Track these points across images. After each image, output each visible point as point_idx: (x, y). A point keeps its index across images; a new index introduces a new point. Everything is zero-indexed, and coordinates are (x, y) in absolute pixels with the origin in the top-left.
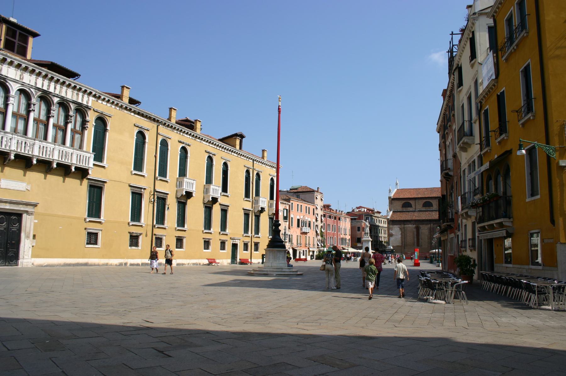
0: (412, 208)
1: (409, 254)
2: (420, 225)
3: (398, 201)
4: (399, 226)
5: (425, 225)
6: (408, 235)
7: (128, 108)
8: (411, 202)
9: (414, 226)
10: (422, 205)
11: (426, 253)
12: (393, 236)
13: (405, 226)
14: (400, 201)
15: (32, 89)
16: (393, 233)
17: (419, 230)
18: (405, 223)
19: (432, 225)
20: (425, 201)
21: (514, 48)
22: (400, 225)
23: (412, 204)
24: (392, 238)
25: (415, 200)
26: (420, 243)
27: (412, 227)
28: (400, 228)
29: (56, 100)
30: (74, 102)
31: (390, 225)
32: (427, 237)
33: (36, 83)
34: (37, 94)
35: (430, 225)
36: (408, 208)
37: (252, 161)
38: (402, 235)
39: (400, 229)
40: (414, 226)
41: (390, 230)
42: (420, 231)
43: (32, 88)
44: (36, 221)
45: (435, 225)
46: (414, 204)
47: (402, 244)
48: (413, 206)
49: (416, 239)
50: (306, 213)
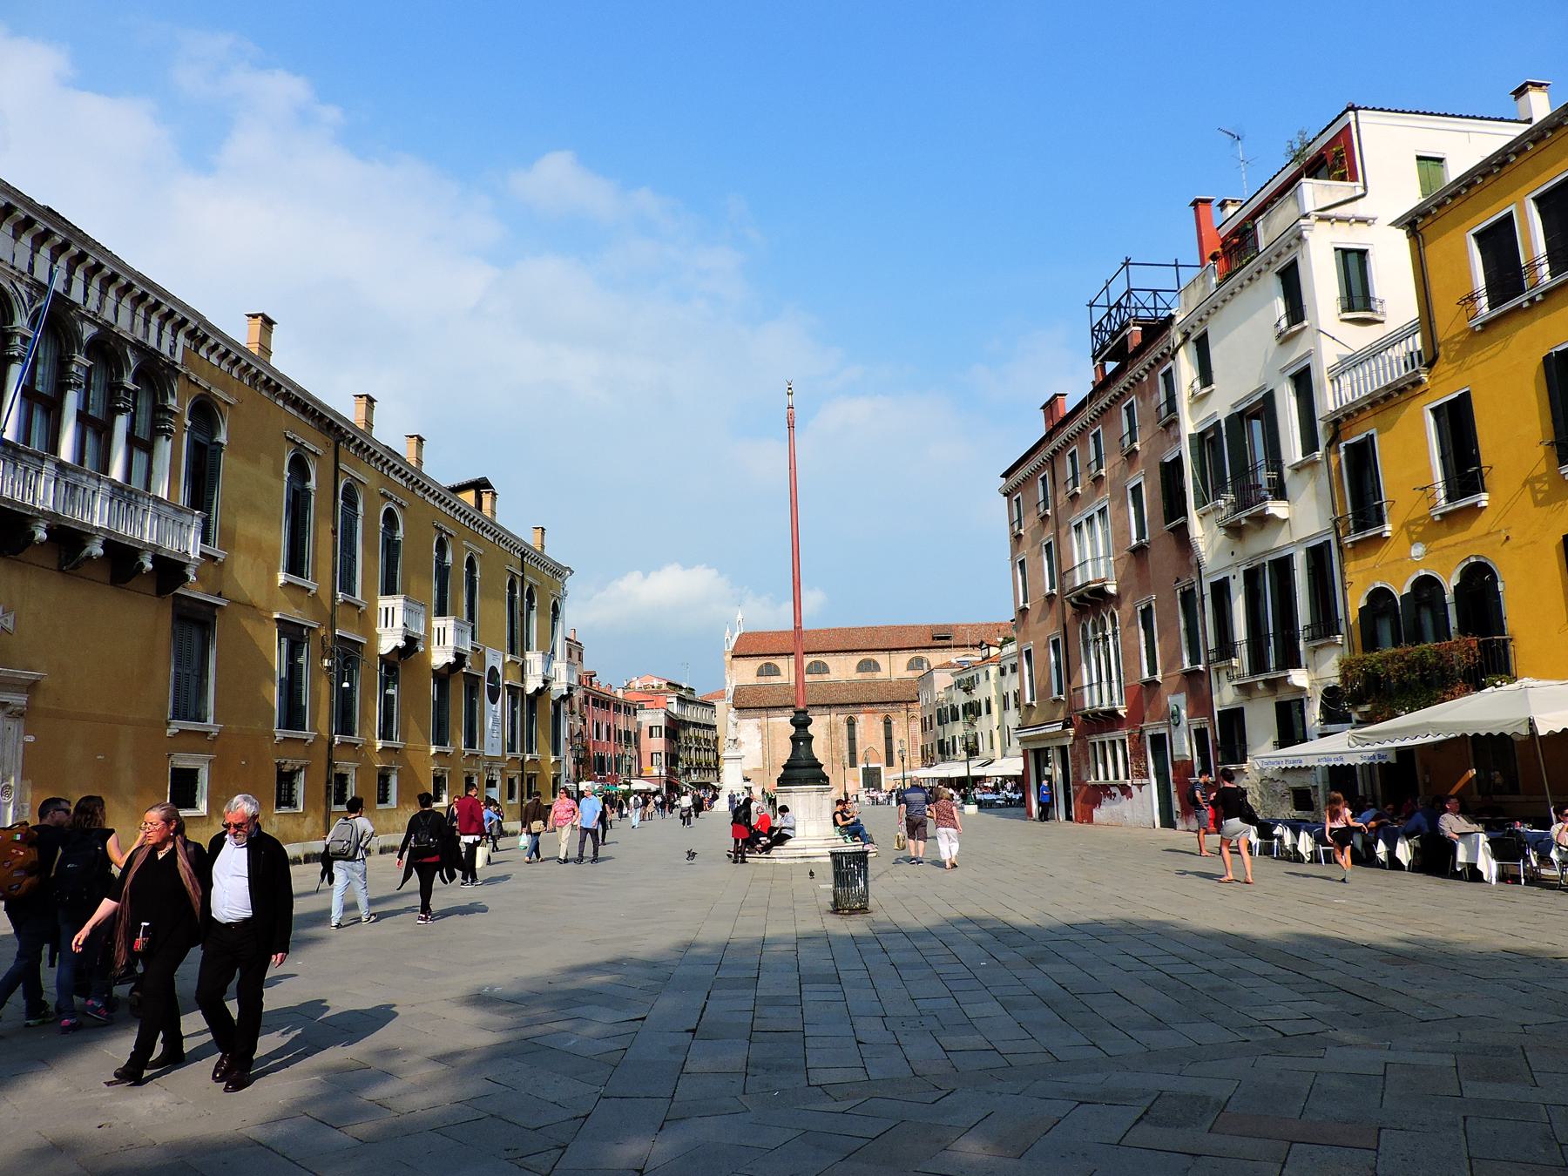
7: (273, 383)
15: (18, 285)
21: (1532, 300)
29: (88, 331)
30: (139, 347)
32: (822, 746)
33: (31, 267)
34: (34, 304)
37: (520, 556)
43: (21, 280)
44: (30, 739)
48: (782, 672)
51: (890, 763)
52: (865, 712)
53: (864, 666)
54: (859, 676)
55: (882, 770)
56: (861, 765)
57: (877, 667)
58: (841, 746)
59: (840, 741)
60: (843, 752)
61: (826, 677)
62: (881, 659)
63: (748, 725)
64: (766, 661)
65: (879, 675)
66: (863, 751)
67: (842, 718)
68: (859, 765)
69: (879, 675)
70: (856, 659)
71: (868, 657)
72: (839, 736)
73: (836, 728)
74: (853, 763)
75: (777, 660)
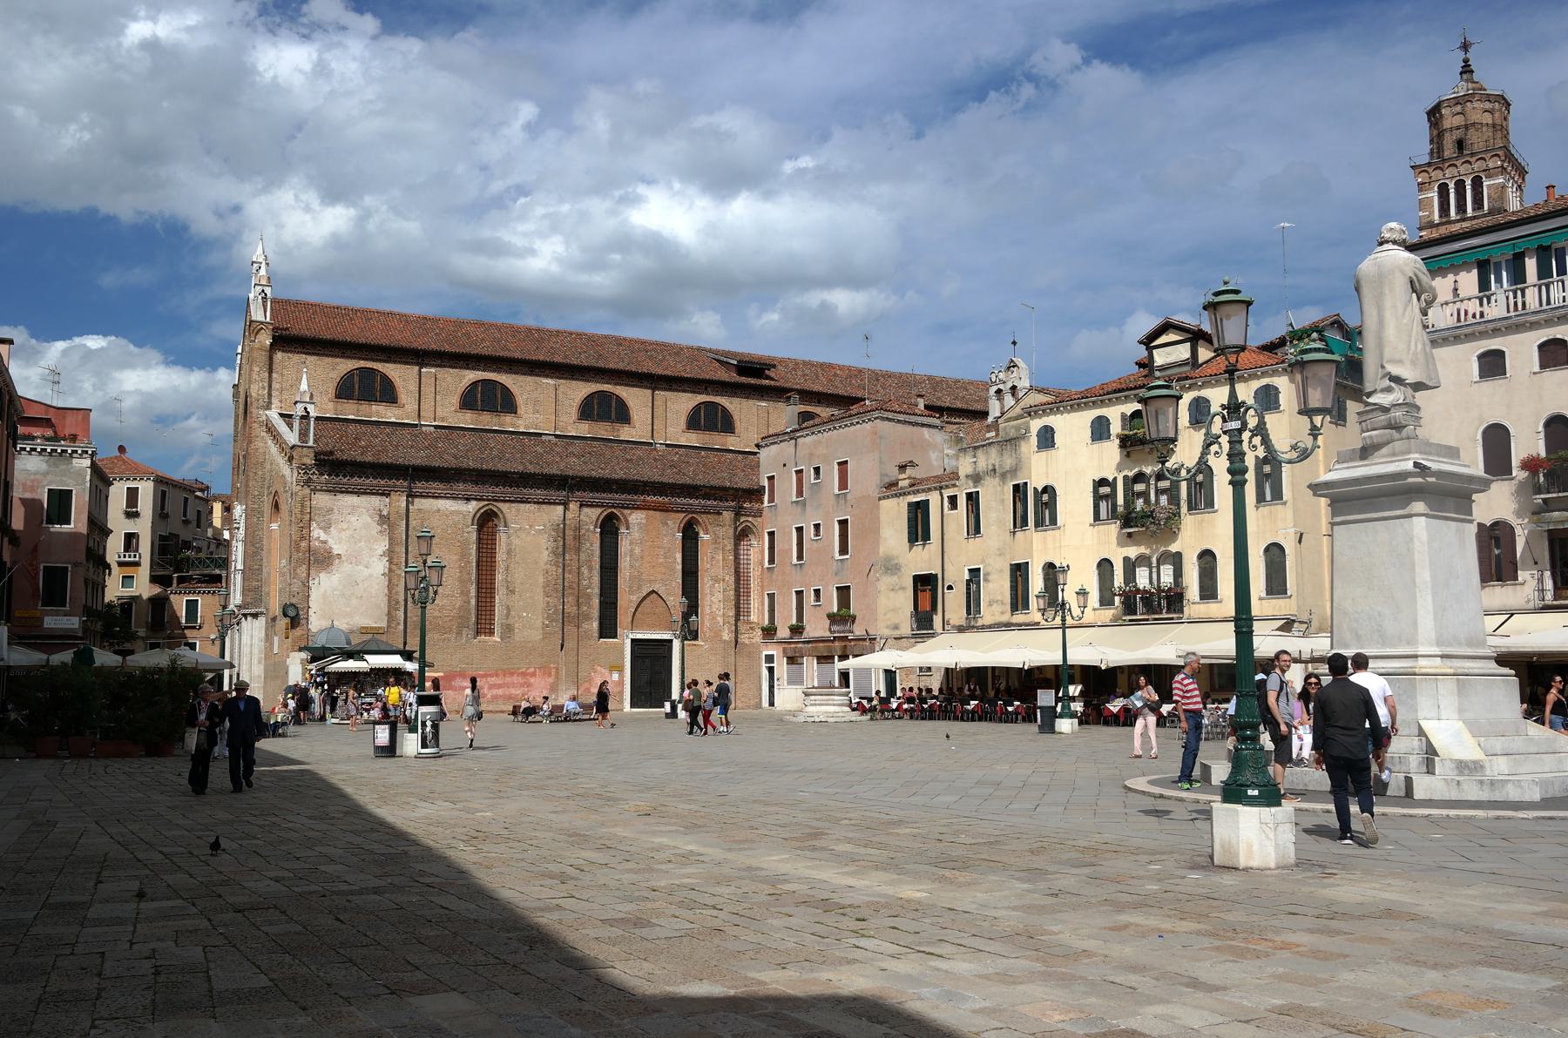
0: (397, 411)
2: (504, 507)
4: (375, 501)
5: (533, 507)
8: (393, 371)
9: (473, 506)
10: (455, 400)
11: (533, 675)
13: (419, 503)
16: (331, 542)
18: (419, 486)
20: (472, 376)
22: (382, 494)
23: (398, 382)
24: (322, 575)
27: (452, 513)
28: (381, 516)
31: (315, 491)
32: (541, 580)
35: (560, 508)
38: (390, 561)
39: (384, 519)
41: (314, 525)
45: (586, 510)
46: (414, 387)
47: (390, 616)
48: (403, 397)
51: (691, 634)
53: (593, 409)
55: (676, 645)
57: (622, 414)
58: (585, 583)
59: (585, 570)
60: (589, 597)
61: (508, 422)
62: (635, 398)
63: (354, 508)
64: (363, 364)
65: (626, 433)
66: (636, 598)
67: (592, 515)
69: (626, 433)
70: (580, 390)
72: (583, 556)
73: (575, 538)
74: (608, 628)
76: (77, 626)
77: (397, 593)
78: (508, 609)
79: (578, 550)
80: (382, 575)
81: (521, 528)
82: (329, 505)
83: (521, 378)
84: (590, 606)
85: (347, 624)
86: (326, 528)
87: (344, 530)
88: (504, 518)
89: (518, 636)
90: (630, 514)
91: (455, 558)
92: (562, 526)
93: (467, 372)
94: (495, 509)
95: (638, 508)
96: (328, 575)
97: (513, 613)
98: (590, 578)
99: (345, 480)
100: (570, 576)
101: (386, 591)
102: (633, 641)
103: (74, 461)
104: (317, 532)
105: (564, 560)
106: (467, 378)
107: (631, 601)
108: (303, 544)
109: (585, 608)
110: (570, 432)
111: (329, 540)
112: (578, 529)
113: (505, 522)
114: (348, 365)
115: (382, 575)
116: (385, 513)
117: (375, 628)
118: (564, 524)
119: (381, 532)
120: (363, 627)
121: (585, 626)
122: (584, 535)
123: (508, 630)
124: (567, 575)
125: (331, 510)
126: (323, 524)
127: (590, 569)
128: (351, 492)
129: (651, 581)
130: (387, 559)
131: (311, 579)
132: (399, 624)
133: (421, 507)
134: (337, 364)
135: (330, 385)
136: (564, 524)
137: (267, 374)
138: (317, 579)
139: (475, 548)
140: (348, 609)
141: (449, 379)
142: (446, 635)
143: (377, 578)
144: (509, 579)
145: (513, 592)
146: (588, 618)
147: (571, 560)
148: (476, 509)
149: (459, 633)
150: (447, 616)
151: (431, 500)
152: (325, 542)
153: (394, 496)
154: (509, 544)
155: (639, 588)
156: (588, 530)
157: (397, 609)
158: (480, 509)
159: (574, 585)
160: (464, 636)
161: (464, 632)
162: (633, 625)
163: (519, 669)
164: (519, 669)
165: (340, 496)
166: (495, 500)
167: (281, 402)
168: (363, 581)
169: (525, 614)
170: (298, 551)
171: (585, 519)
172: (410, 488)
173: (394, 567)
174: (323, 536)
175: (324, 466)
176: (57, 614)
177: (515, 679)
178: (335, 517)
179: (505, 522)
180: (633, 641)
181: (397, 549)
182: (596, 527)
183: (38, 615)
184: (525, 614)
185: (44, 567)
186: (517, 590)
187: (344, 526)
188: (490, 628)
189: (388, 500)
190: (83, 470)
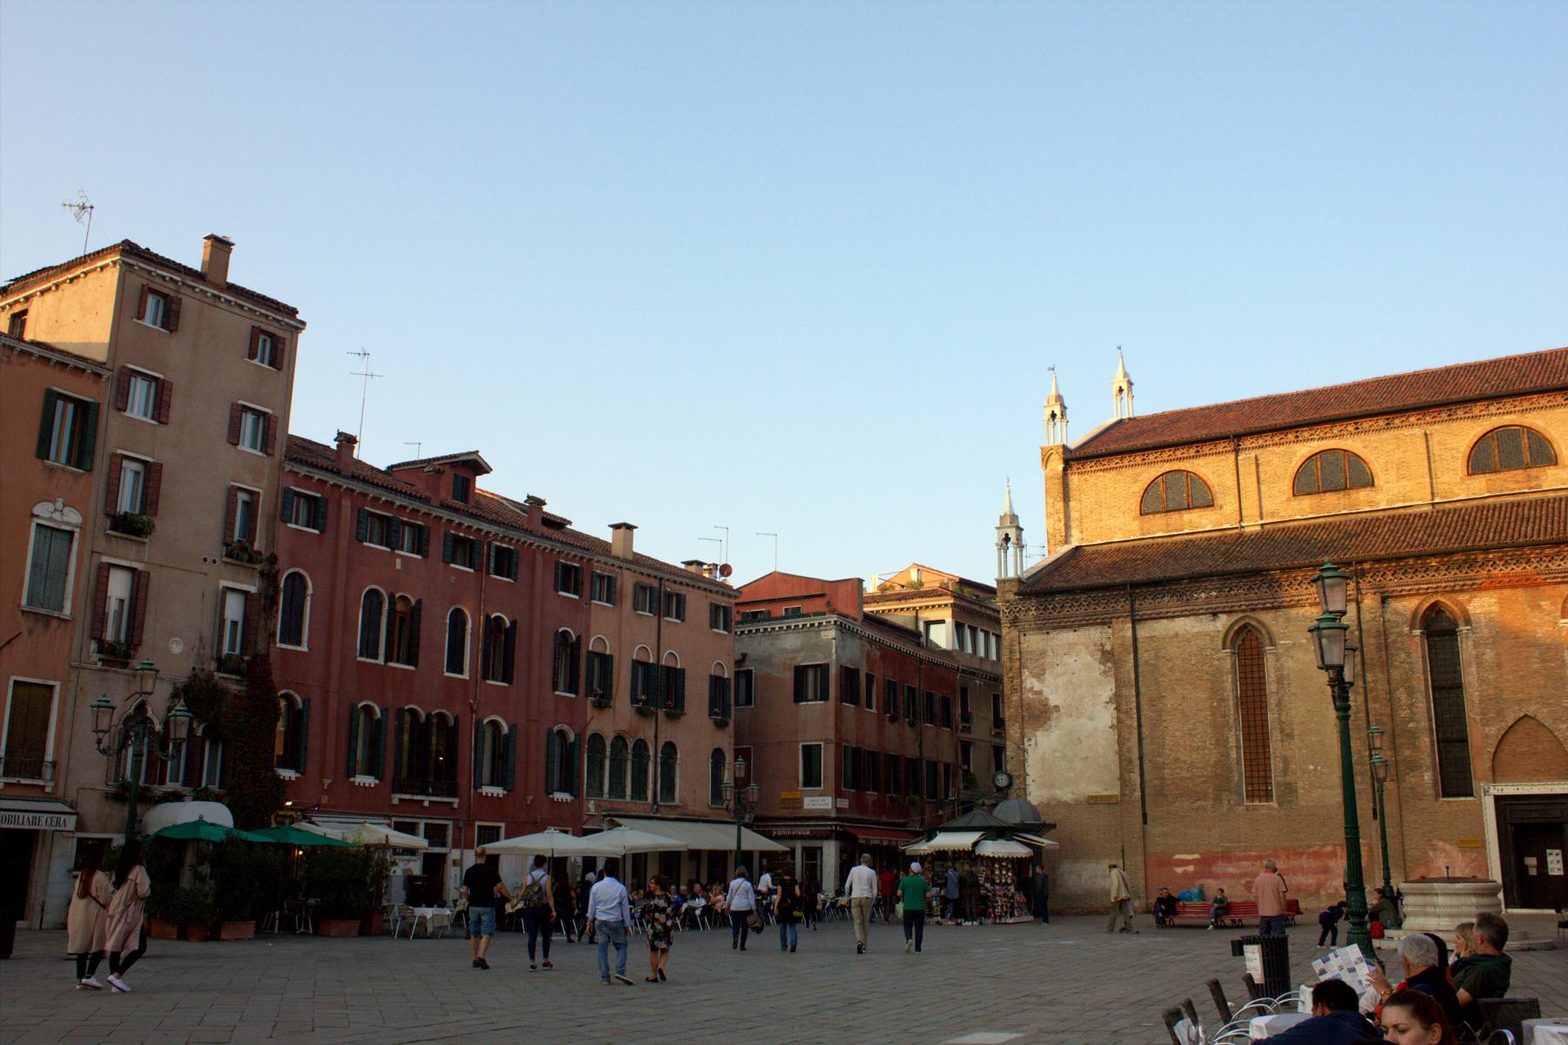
1: (1187, 863)
3: (1110, 475)
4: (1095, 634)
6: (1170, 702)
9: (1223, 622)
10: (1286, 486)
12: (1055, 715)
13: (1144, 631)
14: (1129, 472)
16: (1047, 692)
17: (1260, 655)
18: (1145, 606)
19: (1369, 602)
22: (1103, 624)
23: (1212, 480)
25: (1237, 451)
26: (1276, 765)
27: (1196, 636)
28: (1104, 652)
36: (1187, 516)
39: (1107, 656)
40: (1223, 622)
41: (1026, 673)
42: (1270, 662)
47: (1123, 780)
49: (1234, 737)
50: (43, 450)
52: (1494, 585)
54: (1480, 487)
56: (1488, 794)
58: (1404, 713)
59: (1401, 695)
60: (1413, 734)
63: (1071, 647)
64: (1167, 467)
66: (1494, 731)
68: (1478, 785)
70: (1460, 434)
71: (1508, 419)
73: (1379, 649)
75: (1200, 462)
76: (830, 807)
77: (1129, 750)
78: (1285, 760)
79: (1386, 665)
80: (1111, 727)
81: (1294, 644)
82: (1041, 645)
83: (1373, 437)
84: (1415, 748)
85: (1073, 793)
86: (1039, 676)
87: (1060, 675)
88: (1268, 633)
89: (1304, 799)
90: (1469, 601)
91: (1203, 696)
92: (1357, 633)
93: (1297, 447)
94: (1254, 623)
95: (1480, 589)
96: (1045, 733)
97: (1293, 767)
98: (1411, 706)
99: (1055, 614)
100: (1377, 706)
101: (1116, 748)
102: (1497, 798)
103: (823, 633)
104: (1030, 682)
105: (1365, 682)
106: (1299, 455)
107: (1486, 736)
108: (1015, 698)
109: (1408, 752)
110: (1459, 495)
111: (1045, 689)
112: (1383, 633)
113: (1271, 640)
114: (1146, 472)
115: (1111, 727)
116: (1108, 647)
117: (1106, 796)
118: (1360, 630)
119: (1105, 672)
120: (1092, 797)
121: (1411, 779)
122: (1395, 642)
123: (1290, 789)
124: (1371, 705)
125: (1043, 653)
126: (1036, 671)
127: (1411, 691)
128: (1065, 627)
129: (1519, 702)
130: (1114, 706)
131: (1026, 739)
132: (1134, 790)
133: (1153, 634)
134: (1139, 474)
135: (1133, 501)
136: (1360, 630)
137: (1060, 505)
138: (1033, 739)
139: (1230, 680)
140: (1072, 775)
141: (1276, 461)
142: (1199, 803)
143: (1103, 732)
144: (1283, 718)
145: (1290, 736)
146: (1414, 766)
147: (1375, 682)
148: (1227, 627)
149: (1217, 799)
150: (1200, 777)
151: (1165, 621)
152: (1039, 693)
153: (1117, 625)
154: (1278, 670)
155: (1500, 713)
156: (1400, 634)
157: (1130, 771)
158: (1232, 626)
159: (1385, 719)
160: (1225, 802)
161: (1224, 797)
162: (1495, 775)
163: (1309, 847)
164: (1309, 847)
165: (1053, 634)
166: (1253, 610)
167: (1082, 532)
168: (1087, 737)
169: (1311, 767)
170: (1010, 708)
171: (1393, 618)
172: (1133, 610)
173: (1123, 716)
174: (1037, 686)
175: (1029, 599)
176: (812, 794)
177: (1304, 862)
178: (1048, 660)
179: (1271, 640)
180: (1497, 798)
181: (1125, 692)
182: (1412, 627)
183: (799, 796)
184: (1311, 767)
185: (803, 746)
186: (1296, 732)
187: (1060, 669)
188: (1267, 790)
189: (1110, 631)
190: (828, 643)
